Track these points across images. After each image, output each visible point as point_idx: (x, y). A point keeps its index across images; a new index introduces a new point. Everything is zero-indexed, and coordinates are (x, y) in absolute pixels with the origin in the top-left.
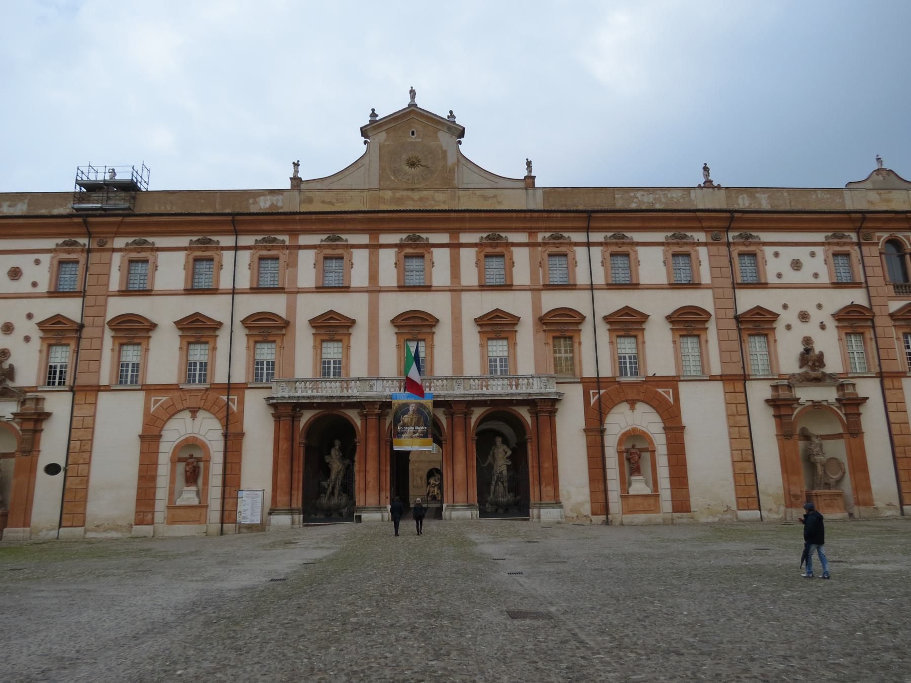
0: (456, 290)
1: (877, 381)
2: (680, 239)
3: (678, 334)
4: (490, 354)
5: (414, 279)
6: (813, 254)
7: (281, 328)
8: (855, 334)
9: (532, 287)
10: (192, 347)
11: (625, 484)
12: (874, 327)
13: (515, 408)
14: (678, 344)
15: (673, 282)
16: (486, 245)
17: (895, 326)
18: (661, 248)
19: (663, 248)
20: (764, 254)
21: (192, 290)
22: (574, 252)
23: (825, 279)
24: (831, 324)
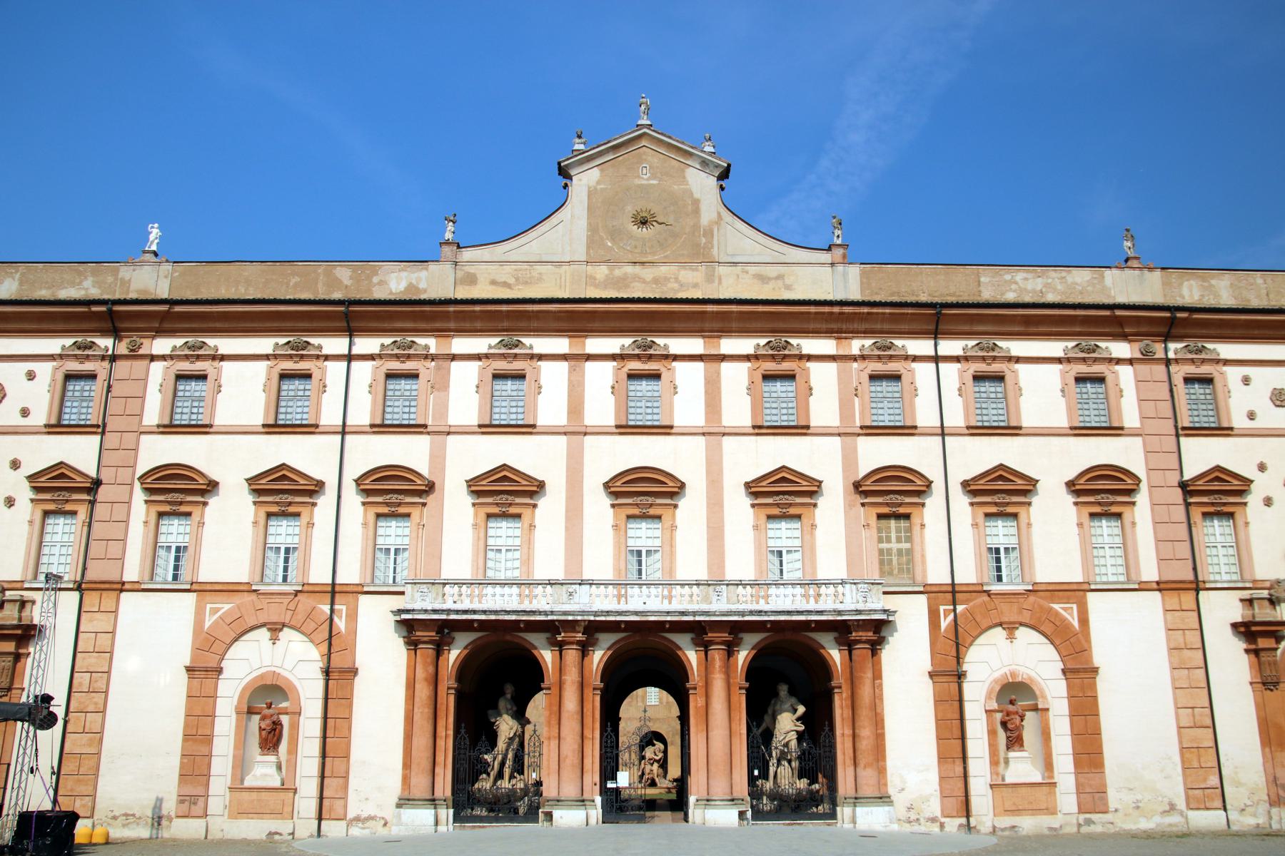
0: (576, 431)
1: (124, 595)
2: (299, 351)
3: (764, 512)
4: (631, 542)
5: (293, 413)
6: (31, 376)
7: (203, 492)
8: (1219, 514)
9: (705, 430)
10: (165, 521)
11: (241, 766)
12: (92, 503)
13: (521, 634)
14: (981, 528)
15: (973, 423)
16: (179, 358)
17: (863, 505)
18: (746, 366)
19: (958, 366)
20: (1117, 378)
21: (171, 426)
22: (807, 370)
23: (40, 417)
24: (24, 494)
